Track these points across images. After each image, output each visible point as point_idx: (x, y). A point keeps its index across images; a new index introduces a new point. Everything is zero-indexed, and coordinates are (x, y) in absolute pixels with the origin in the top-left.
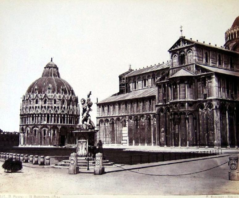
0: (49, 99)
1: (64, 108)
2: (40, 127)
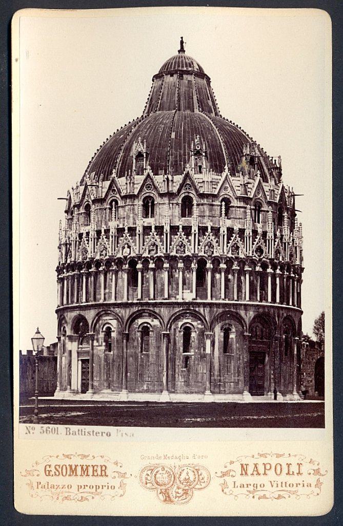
0: (202, 196)
1: (264, 234)
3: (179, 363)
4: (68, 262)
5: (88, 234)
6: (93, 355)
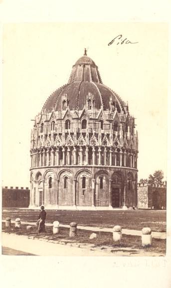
1: (119, 136)
2: (75, 170)
3: (81, 192)
4: (34, 148)
5: (42, 136)
6: (44, 190)
